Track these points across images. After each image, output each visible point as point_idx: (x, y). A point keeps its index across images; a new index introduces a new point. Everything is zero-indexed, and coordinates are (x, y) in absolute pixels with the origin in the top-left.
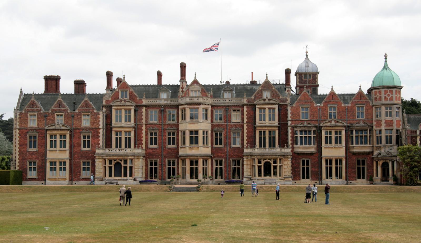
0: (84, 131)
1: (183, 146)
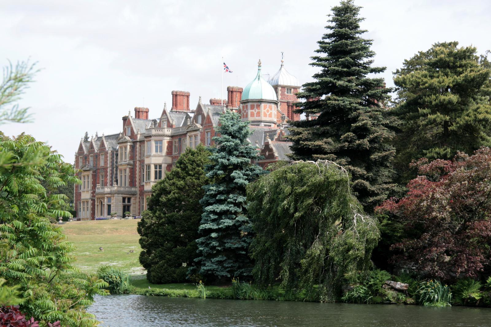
0: (101, 171)
1: (148, 181)
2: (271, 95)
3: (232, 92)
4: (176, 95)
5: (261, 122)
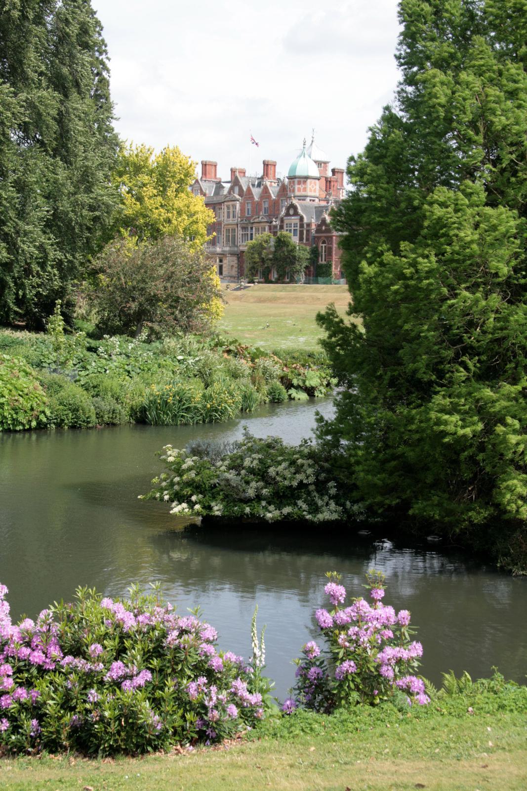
2: (314, 171)
3: (267, 165)
4: (206, 165)
5: (307, 196)
